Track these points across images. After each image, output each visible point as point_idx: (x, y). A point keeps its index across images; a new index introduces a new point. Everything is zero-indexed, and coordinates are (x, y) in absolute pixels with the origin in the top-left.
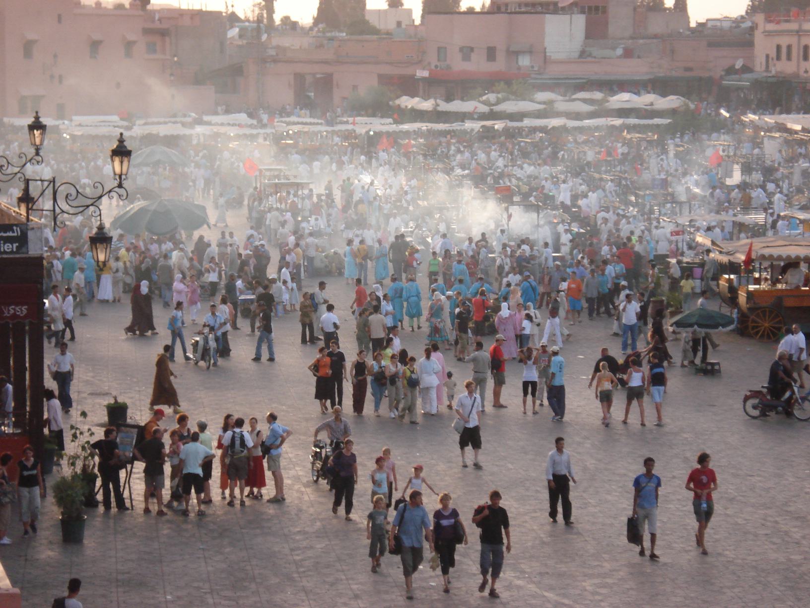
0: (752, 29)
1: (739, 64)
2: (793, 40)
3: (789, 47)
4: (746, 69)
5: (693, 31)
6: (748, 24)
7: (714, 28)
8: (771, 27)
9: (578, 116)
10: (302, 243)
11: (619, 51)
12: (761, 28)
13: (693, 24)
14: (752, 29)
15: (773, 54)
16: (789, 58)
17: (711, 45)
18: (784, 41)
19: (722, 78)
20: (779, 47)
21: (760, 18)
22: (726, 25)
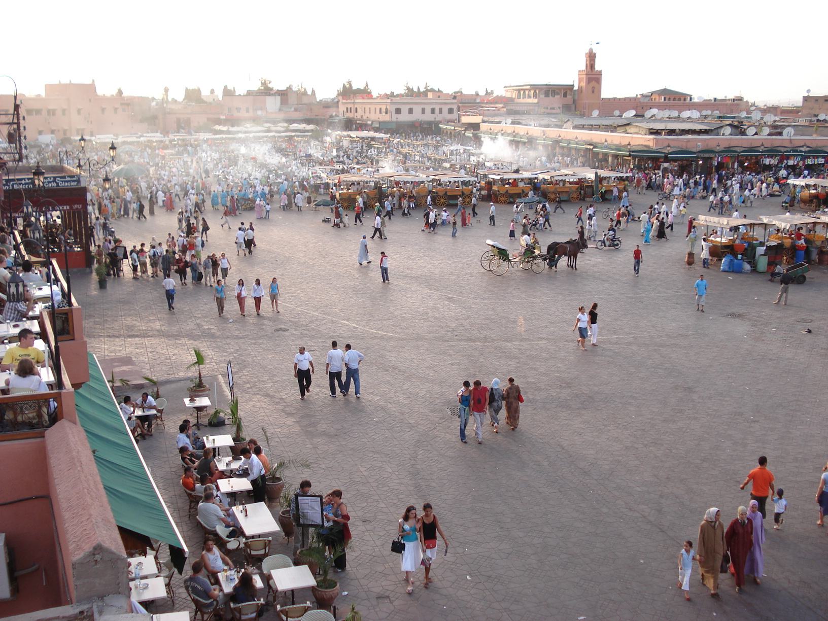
0: (338, 102)
1: (334, 114)
2: (352, 106)
3: (351, 108)
4: (336, 116)
5: (318, 102)
6: (337, 100)
7: (325, 101)
8: (344, 101)
9: (279, 132)
10: (102, 170)
11: (293, 109)
12: (341, 102)
13: (318, 100)
14: (338, 102)
15: (345, 110)
16: (351, 112)
17: (324, 107)
18: (349, 106)
19: (328, 119)
20: (347, 108)
21: (340, 98)
22: (329, 100)
